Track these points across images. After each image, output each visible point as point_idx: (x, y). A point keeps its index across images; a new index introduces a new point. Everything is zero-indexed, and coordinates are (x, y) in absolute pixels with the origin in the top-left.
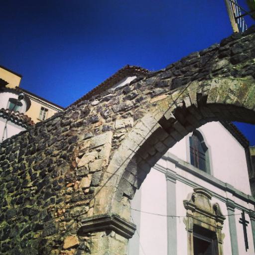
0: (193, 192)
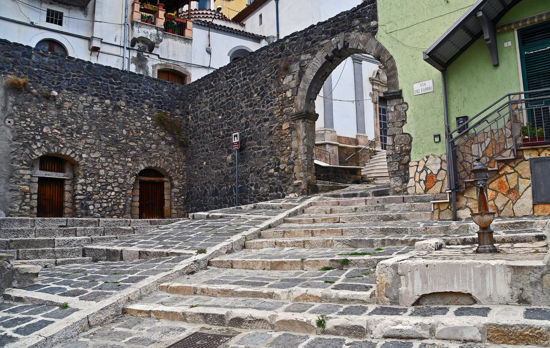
0: (378, 69)
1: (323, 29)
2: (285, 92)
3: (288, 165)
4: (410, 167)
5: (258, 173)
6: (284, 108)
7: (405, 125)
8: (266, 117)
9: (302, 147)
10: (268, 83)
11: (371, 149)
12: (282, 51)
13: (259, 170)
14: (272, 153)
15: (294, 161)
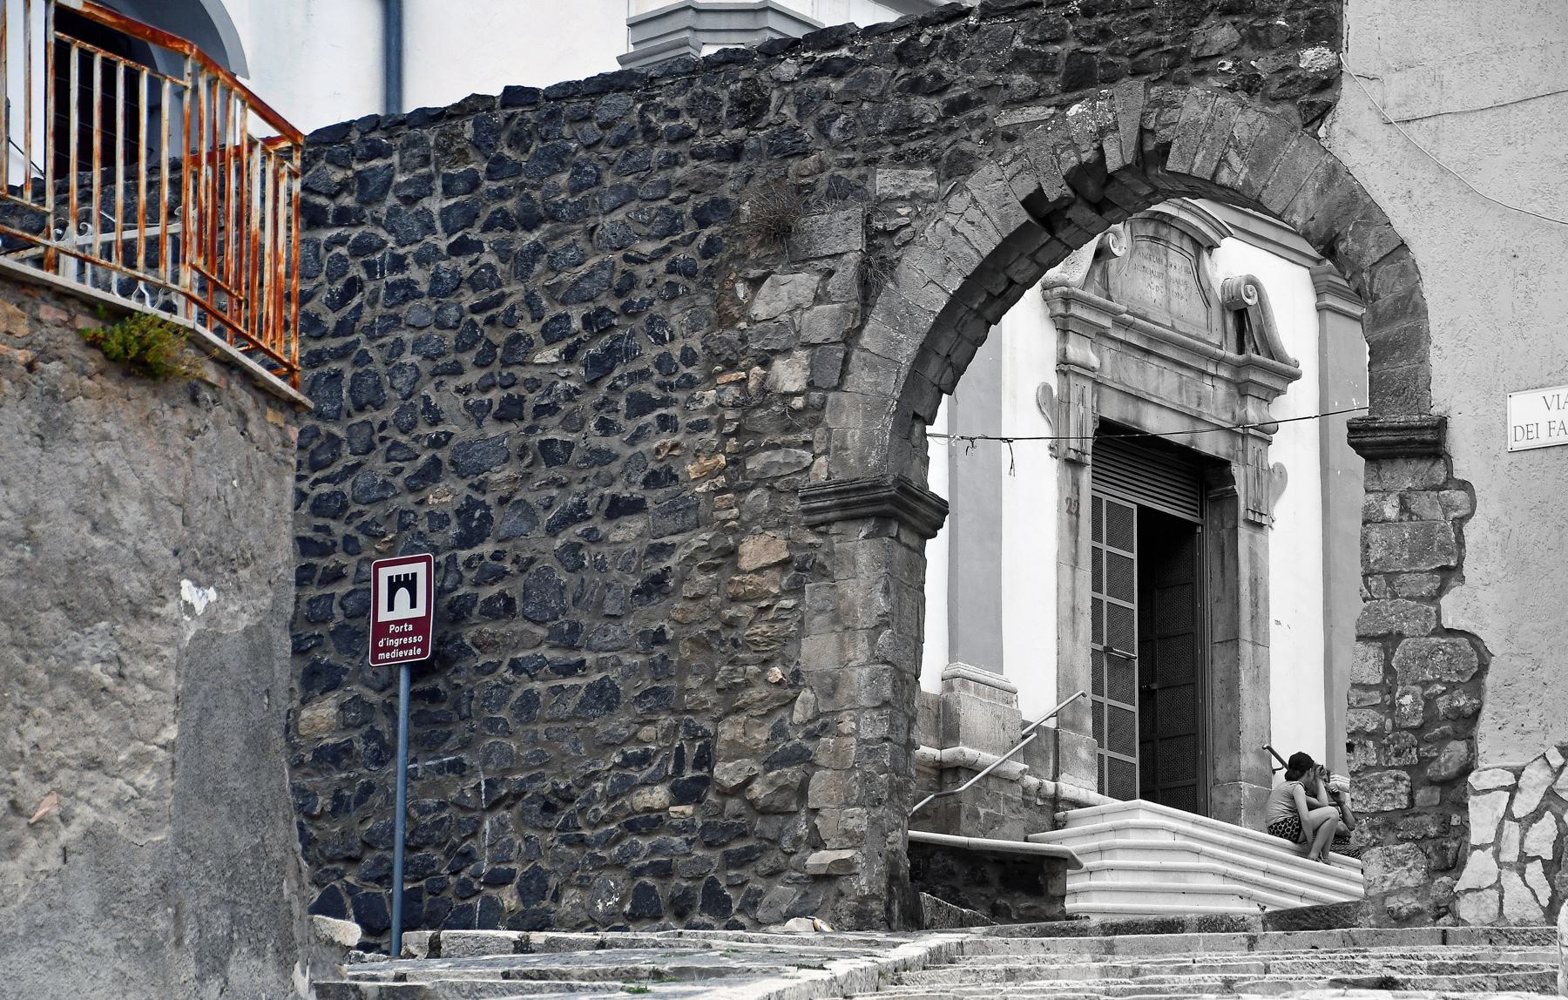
1: (1018, 43)
2: (765, 363)
3: (770, 765)
4: (1476, 793)
5: (549, 808)
6: (751, 451)
7: (1457, 589)
8: (617, 489)
9: (866, 671)
10: (647, 294)
11: (1032, 781)
12: (750, 123)
13: (555, 792)
14: (658, 699)
15: (809, 745)
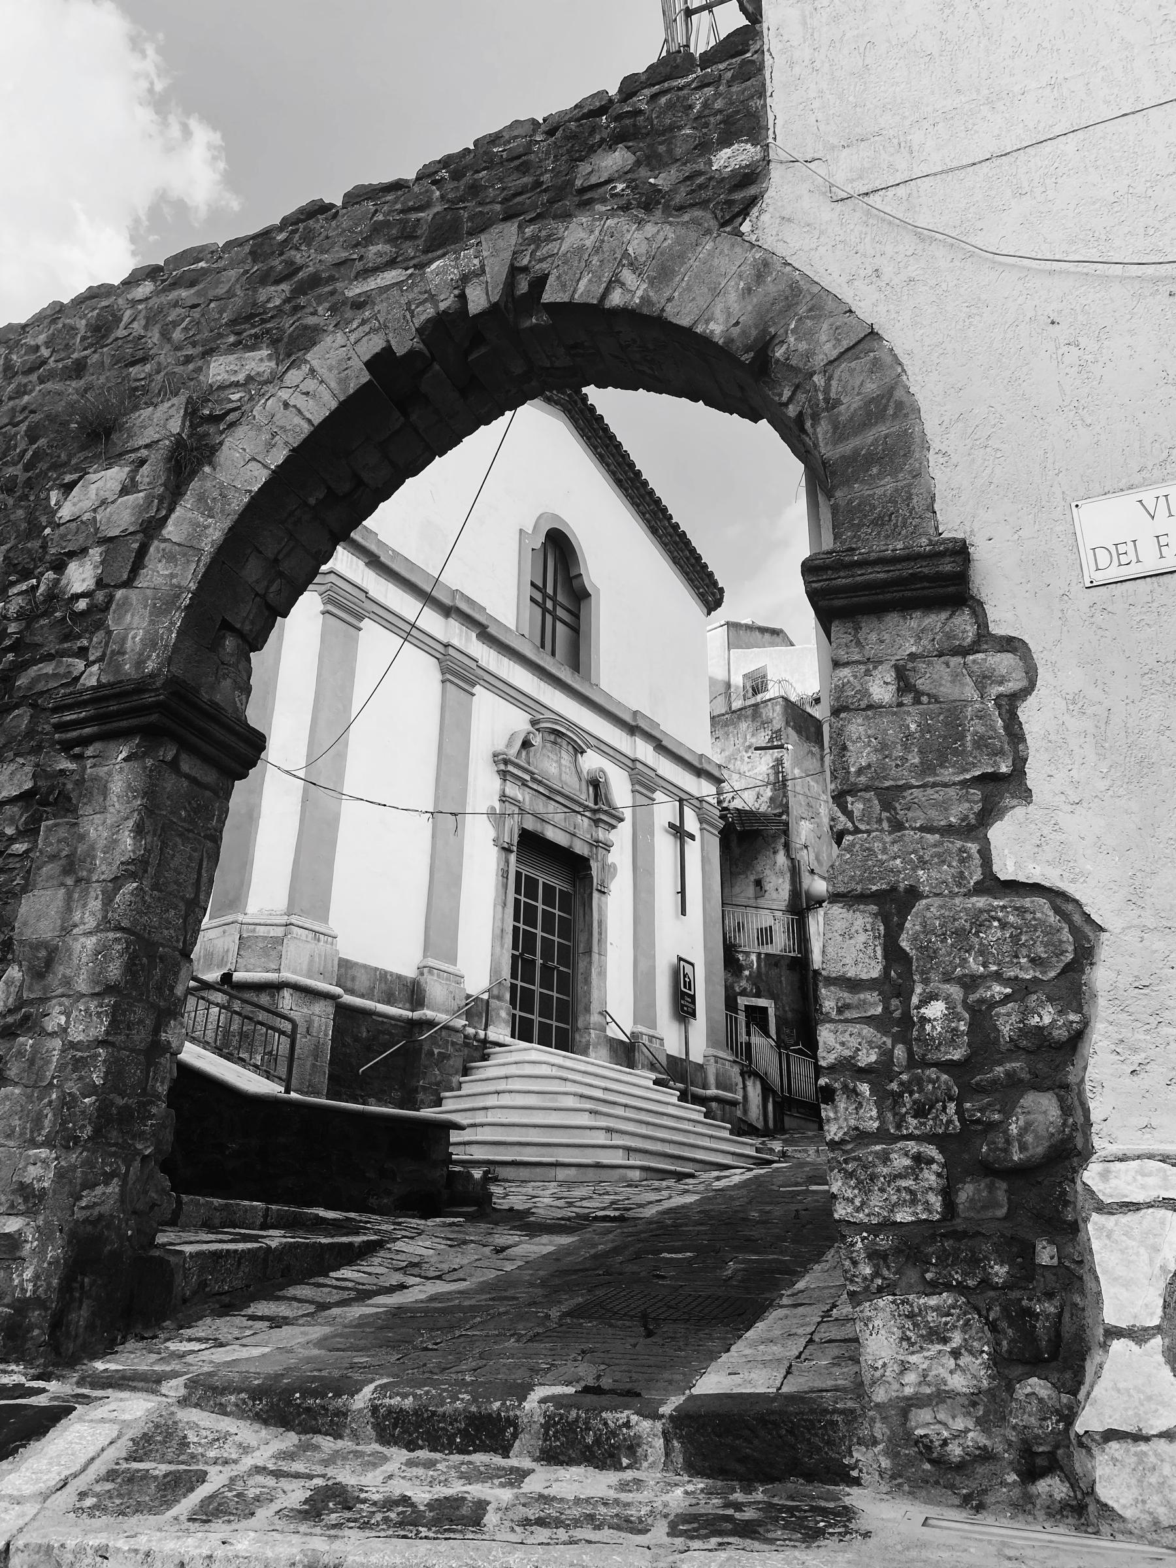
0: (529, 727)
2: (60, 567)
4: (1102, 1208)
11: (471, 1031)
